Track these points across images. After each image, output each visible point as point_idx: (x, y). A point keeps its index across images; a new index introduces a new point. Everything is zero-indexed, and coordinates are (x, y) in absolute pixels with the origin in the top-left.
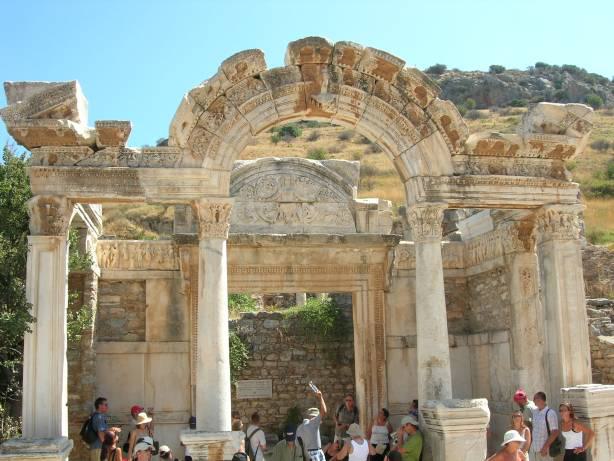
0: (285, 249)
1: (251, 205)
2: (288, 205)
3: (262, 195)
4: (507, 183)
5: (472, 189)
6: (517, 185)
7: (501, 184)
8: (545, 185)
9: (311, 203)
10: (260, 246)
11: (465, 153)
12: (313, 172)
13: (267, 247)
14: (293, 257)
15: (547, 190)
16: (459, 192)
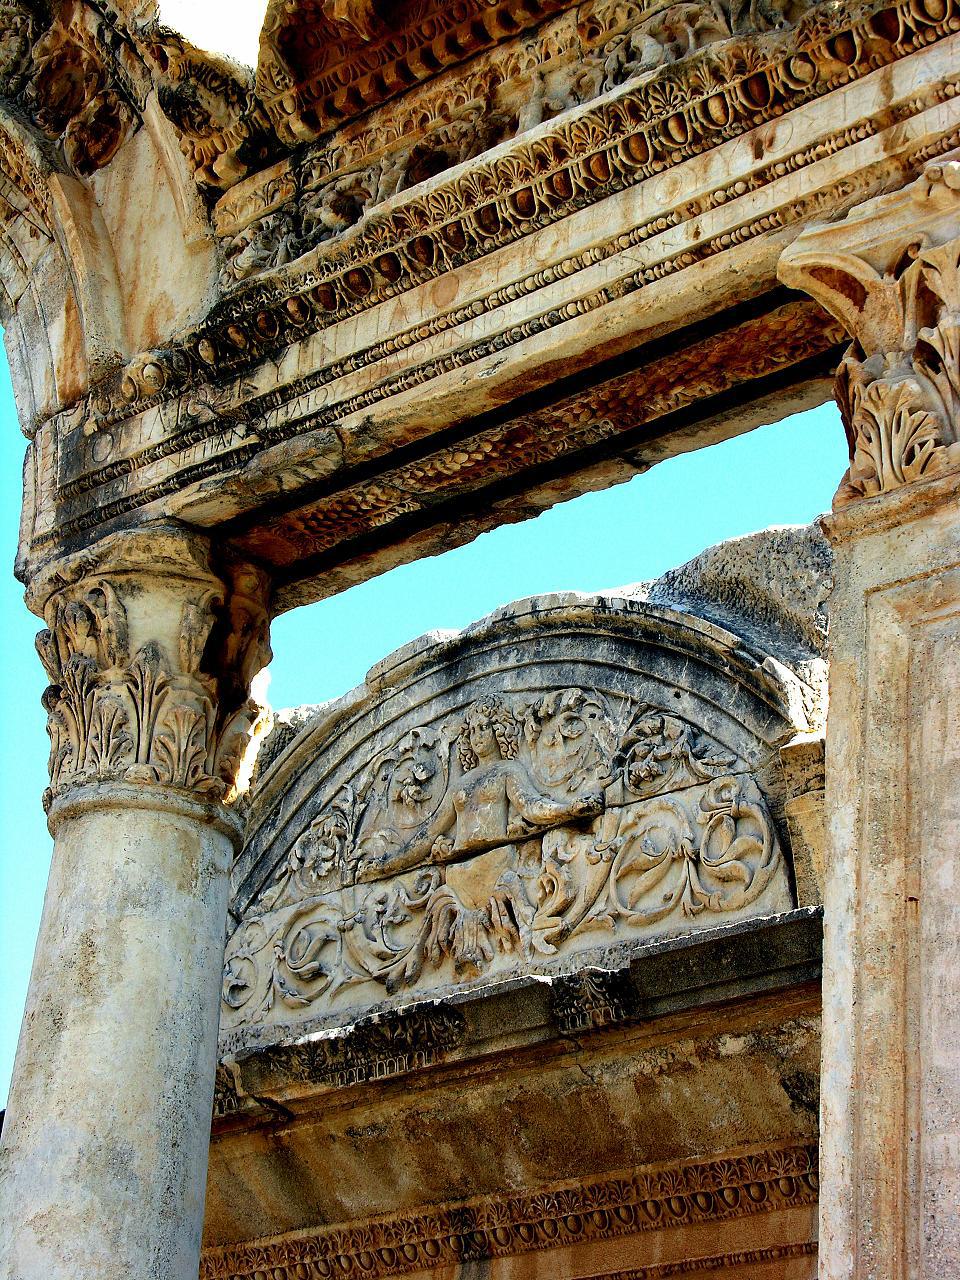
0: (390, 1110)
1: (335, 905)
2: (472, 865)
3: (376, 843)
4: (488, 219)
5: (293, 364)
6: (566, 197)
7: (462, 247)
8: (766, 99)
9: (580, 823)
10: (284, 1115)
11: (260, 150)
12: (602, 653)
13: (317, 1111)
14: (446, 1150)
15: (792, 131)
16: (224, 423)
